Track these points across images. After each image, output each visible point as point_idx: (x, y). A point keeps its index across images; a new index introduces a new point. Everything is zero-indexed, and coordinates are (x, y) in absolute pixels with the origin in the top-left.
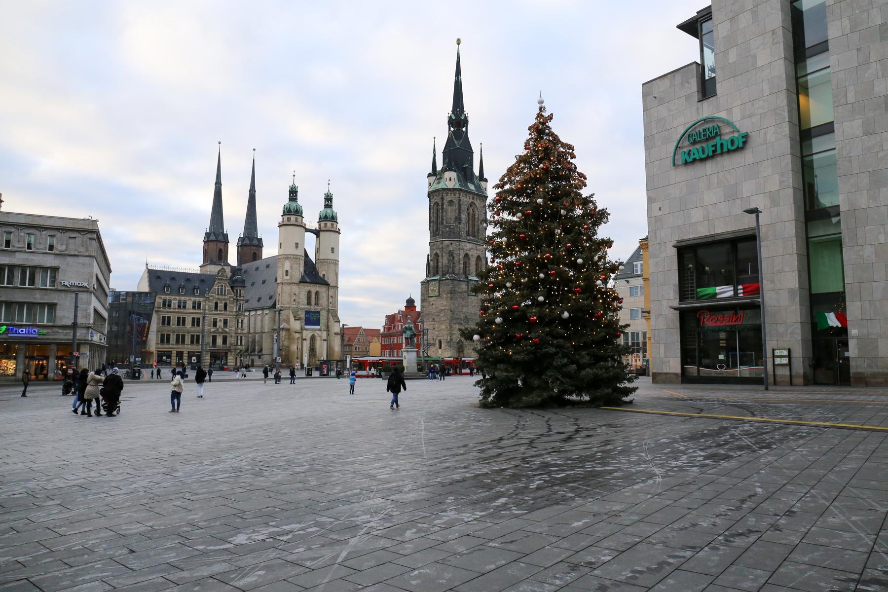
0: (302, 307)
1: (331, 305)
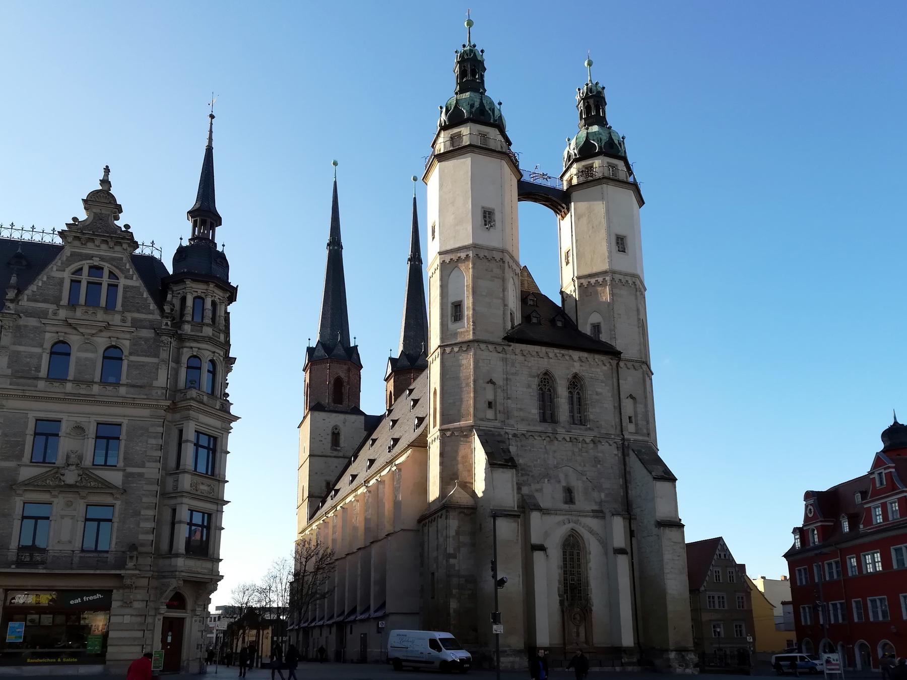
0: (522, 428)
1: (631, 428)
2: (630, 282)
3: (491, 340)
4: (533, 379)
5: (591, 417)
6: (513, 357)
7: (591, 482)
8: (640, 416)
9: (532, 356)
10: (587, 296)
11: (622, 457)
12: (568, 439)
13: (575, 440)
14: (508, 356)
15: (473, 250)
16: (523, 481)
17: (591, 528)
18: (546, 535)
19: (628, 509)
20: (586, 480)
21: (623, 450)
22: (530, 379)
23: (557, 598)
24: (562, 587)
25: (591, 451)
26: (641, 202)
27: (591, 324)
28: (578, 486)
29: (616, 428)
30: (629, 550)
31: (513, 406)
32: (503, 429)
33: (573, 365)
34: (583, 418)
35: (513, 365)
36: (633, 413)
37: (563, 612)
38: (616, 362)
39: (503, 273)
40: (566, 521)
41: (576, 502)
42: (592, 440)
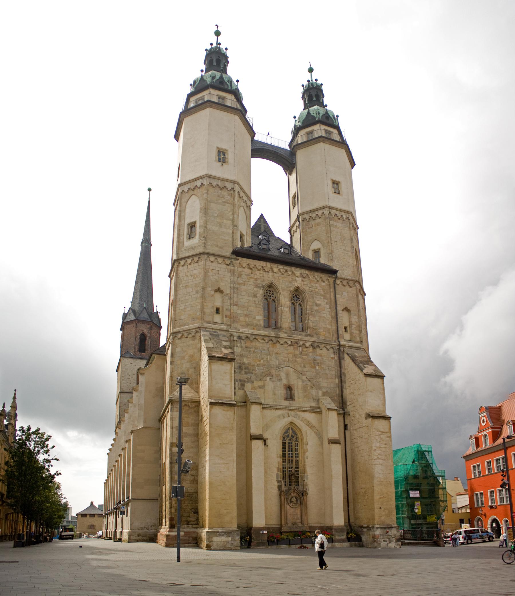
1: (347, 336)
2: (344, 217)
3: (220, 253)
4: (258, 289)
5: (311, 324)
6: (240, 269)
7: (309, 381)
8: (354, 326)
9: (258, 270)
10: (309, 228)
11: (338, 360)
12: (290, 343)
13: (296, 344)
14: (236, 268)
15: (207, 179)
16: (247, 378)
17: (309, 422)
18: (266, 427)
19: (343, 406)
20: (305, 379)
21: (339, 354)
22: (255, 289)
23: (276, 484)
24: (281, 474)
25: (311, 354)
26: (353, 164)
27: (313, 250)
28: (298, 384)
29: (333, 335)
30: (342, 441)
31: (239, 312)
32: (229, 331)
33: (296, 279)
34: (304, 325)
35: (240, 276)
36: (348, 323)
37: (280, 495)
38: (332, 280)
39: (234, 199)
40: (286, 415)
41: (296, 399)
42: (311, 345)
